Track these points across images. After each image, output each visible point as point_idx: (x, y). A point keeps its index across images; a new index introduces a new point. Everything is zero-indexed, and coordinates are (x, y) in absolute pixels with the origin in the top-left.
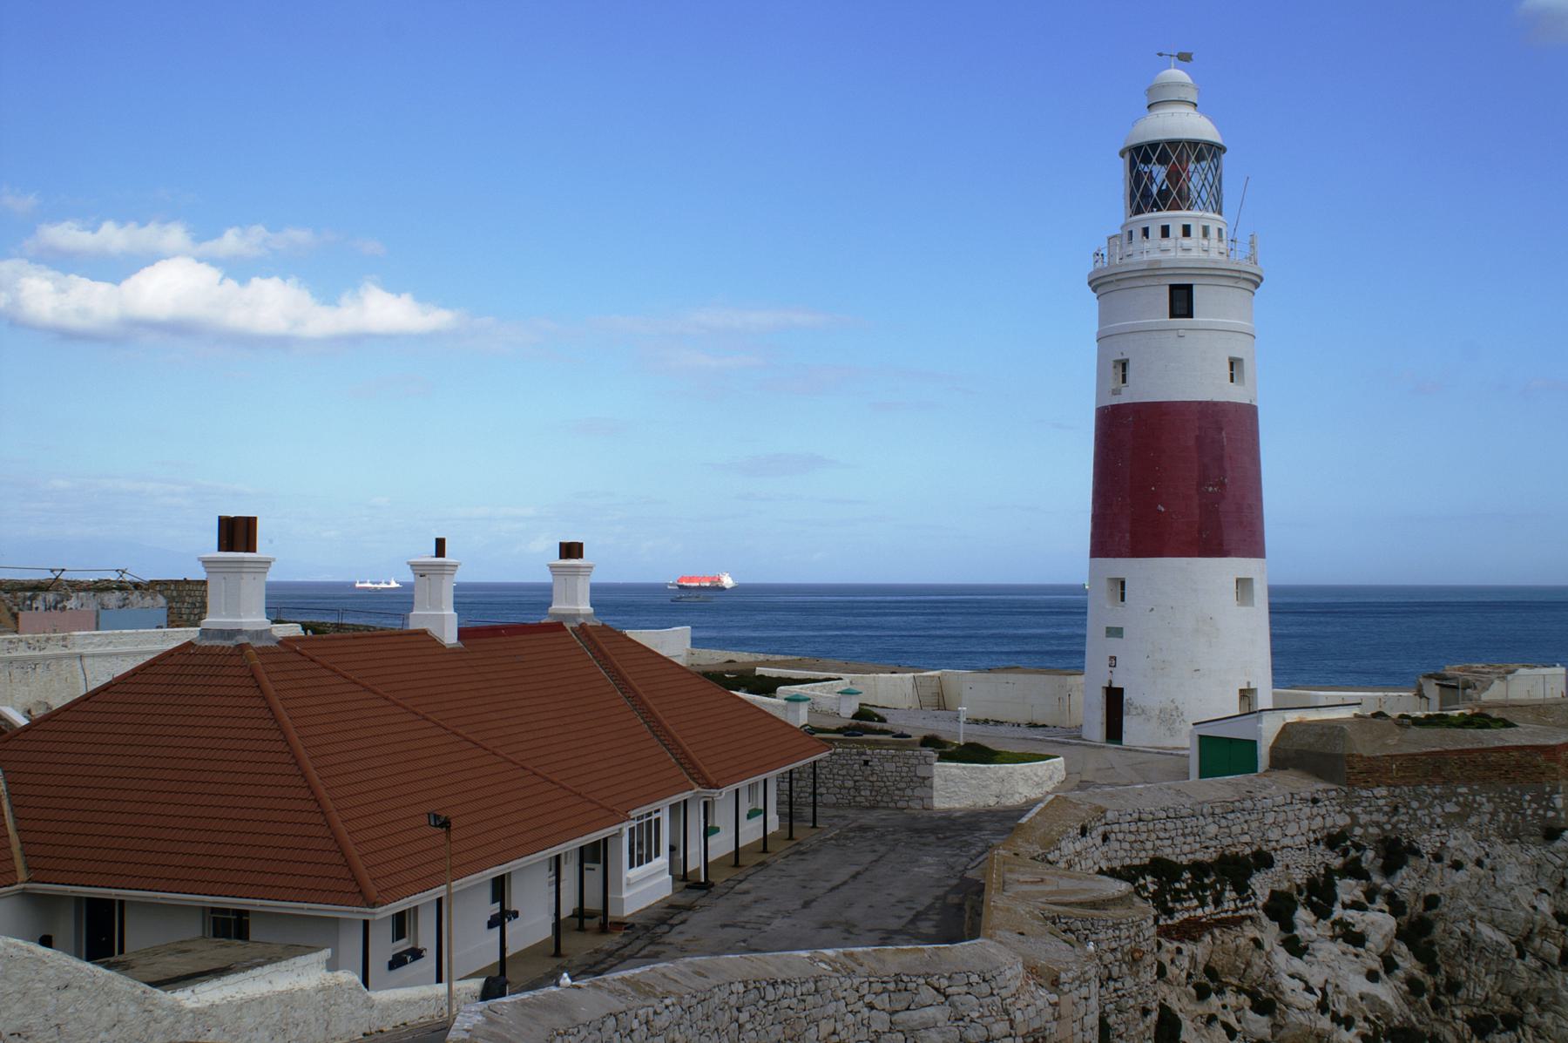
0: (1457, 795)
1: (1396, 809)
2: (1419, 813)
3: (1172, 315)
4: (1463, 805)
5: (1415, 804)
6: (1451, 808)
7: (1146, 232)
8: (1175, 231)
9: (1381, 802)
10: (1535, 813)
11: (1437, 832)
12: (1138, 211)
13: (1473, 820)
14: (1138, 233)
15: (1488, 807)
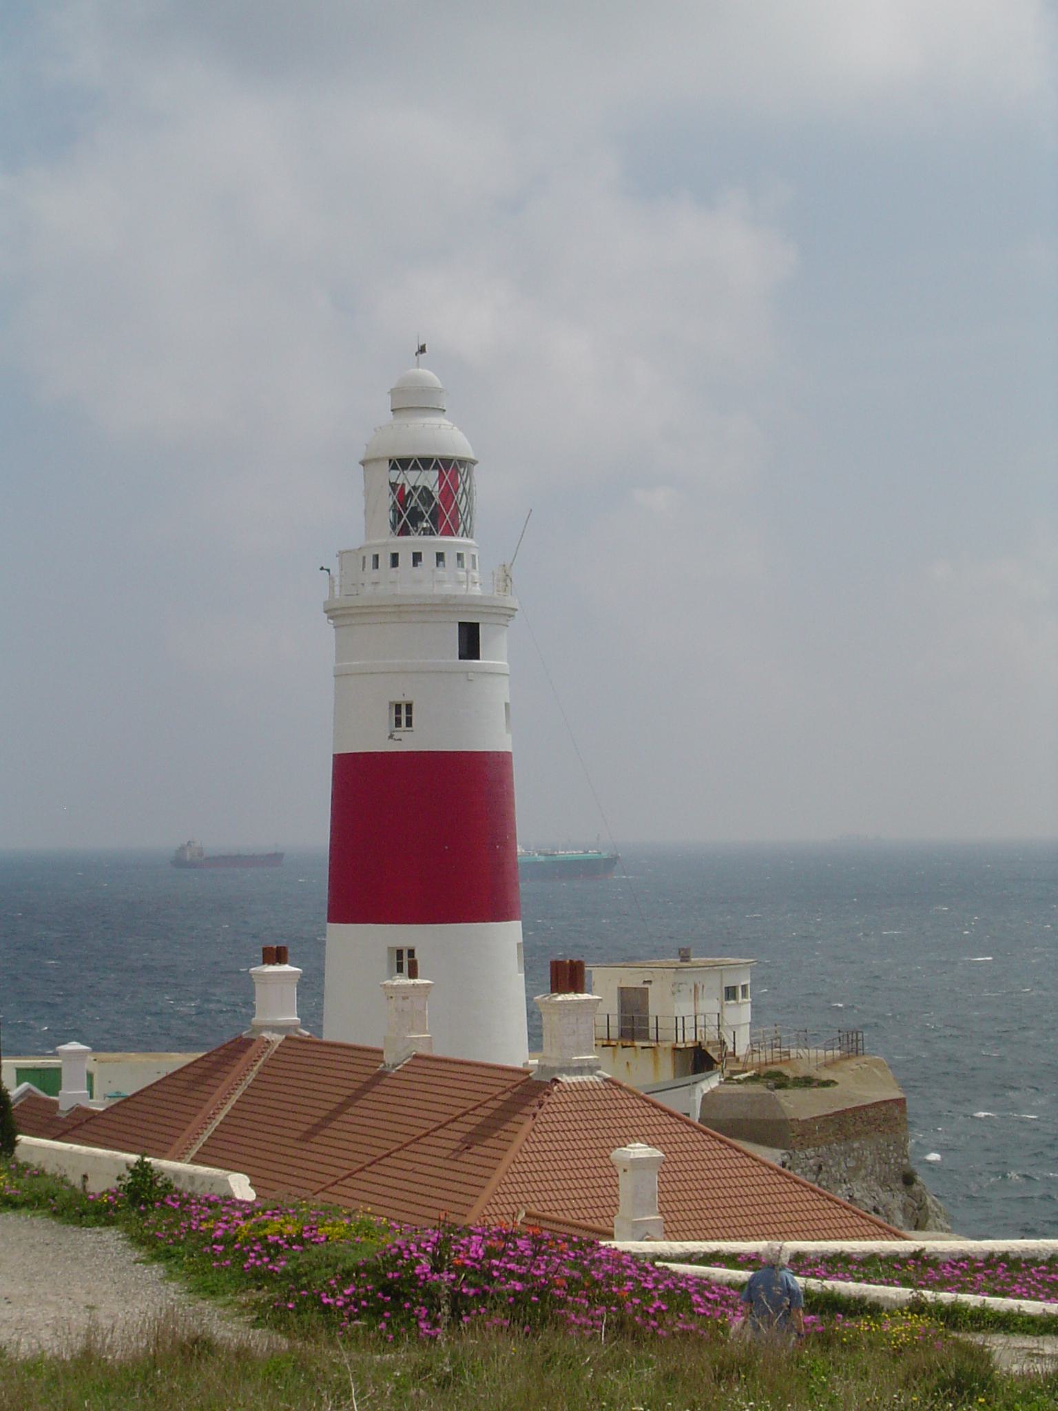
0: (853, 1150)
1: (820, 1168)
2: (833, 1170)
3: (460, 658)
4: (858, 1159)
5: (831, 1162)
6: (852, 1164)
7: (417, 557)
8: (450, 559)
9: (811, 1162)
10: (896, 1162)
11: (844, 1186)
12: (404, 532)
13: (863, 1172)
14: (405, 559)
15: (870, 1158)
